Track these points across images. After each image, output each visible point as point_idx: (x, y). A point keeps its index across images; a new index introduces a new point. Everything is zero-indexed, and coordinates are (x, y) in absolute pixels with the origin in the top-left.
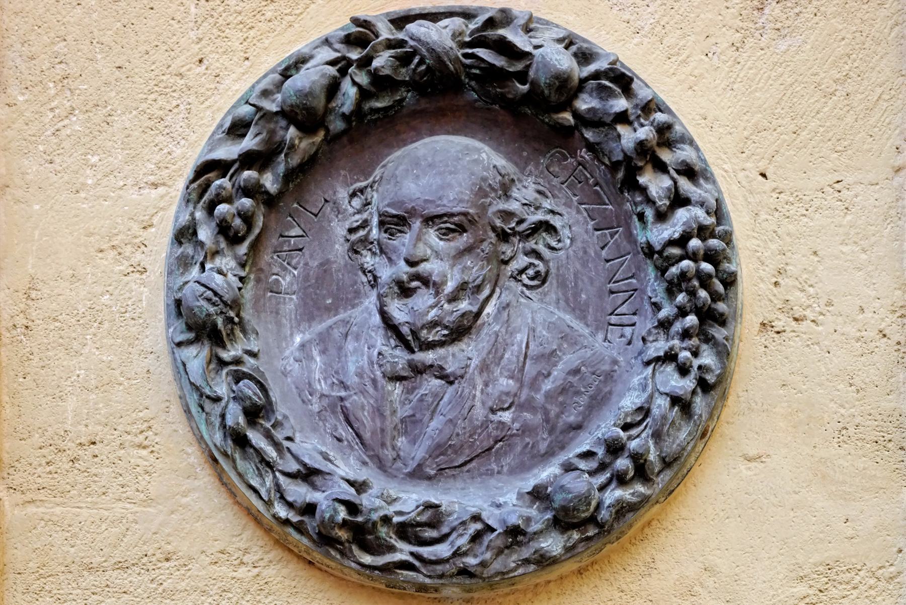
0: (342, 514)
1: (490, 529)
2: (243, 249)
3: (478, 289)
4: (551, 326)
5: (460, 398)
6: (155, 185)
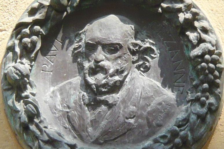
3: (122, 72)
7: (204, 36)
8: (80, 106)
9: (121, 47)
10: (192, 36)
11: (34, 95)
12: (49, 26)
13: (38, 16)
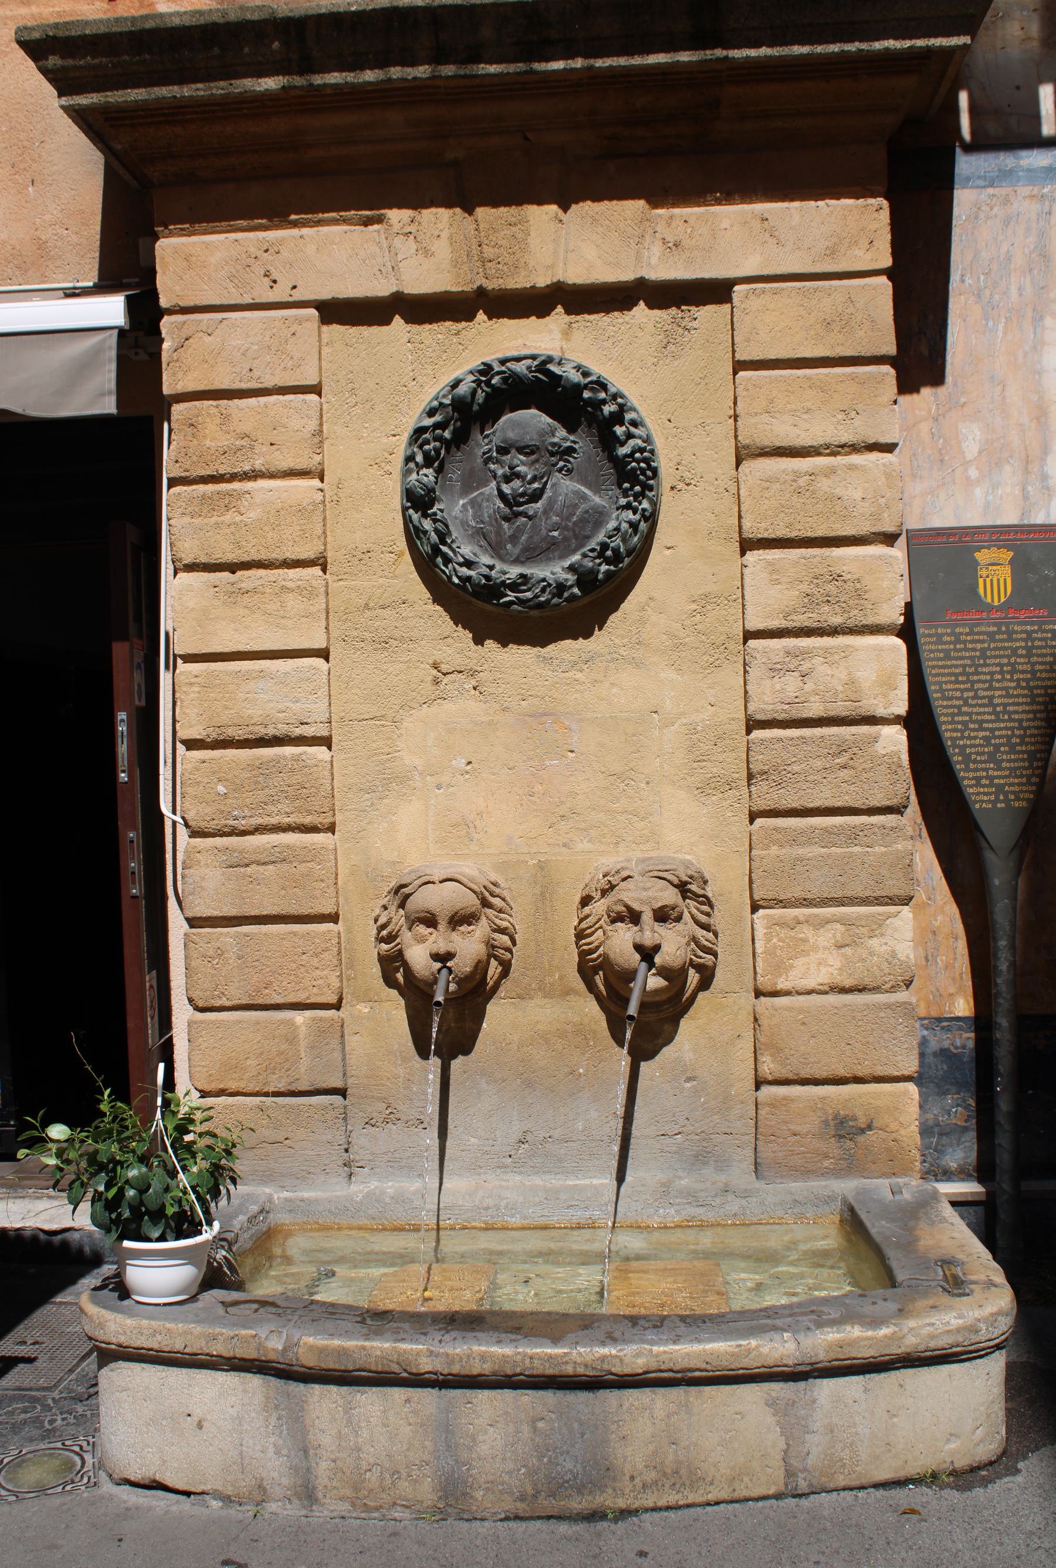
1: (549, 585)
3: (542, 477)
5: (533, 527)
6: (394, 435)
7: (632, 429)
8: (496, 520)
9: (538, 448)
10: (619, 430)
11: (442, 511)
13: (438, 418)
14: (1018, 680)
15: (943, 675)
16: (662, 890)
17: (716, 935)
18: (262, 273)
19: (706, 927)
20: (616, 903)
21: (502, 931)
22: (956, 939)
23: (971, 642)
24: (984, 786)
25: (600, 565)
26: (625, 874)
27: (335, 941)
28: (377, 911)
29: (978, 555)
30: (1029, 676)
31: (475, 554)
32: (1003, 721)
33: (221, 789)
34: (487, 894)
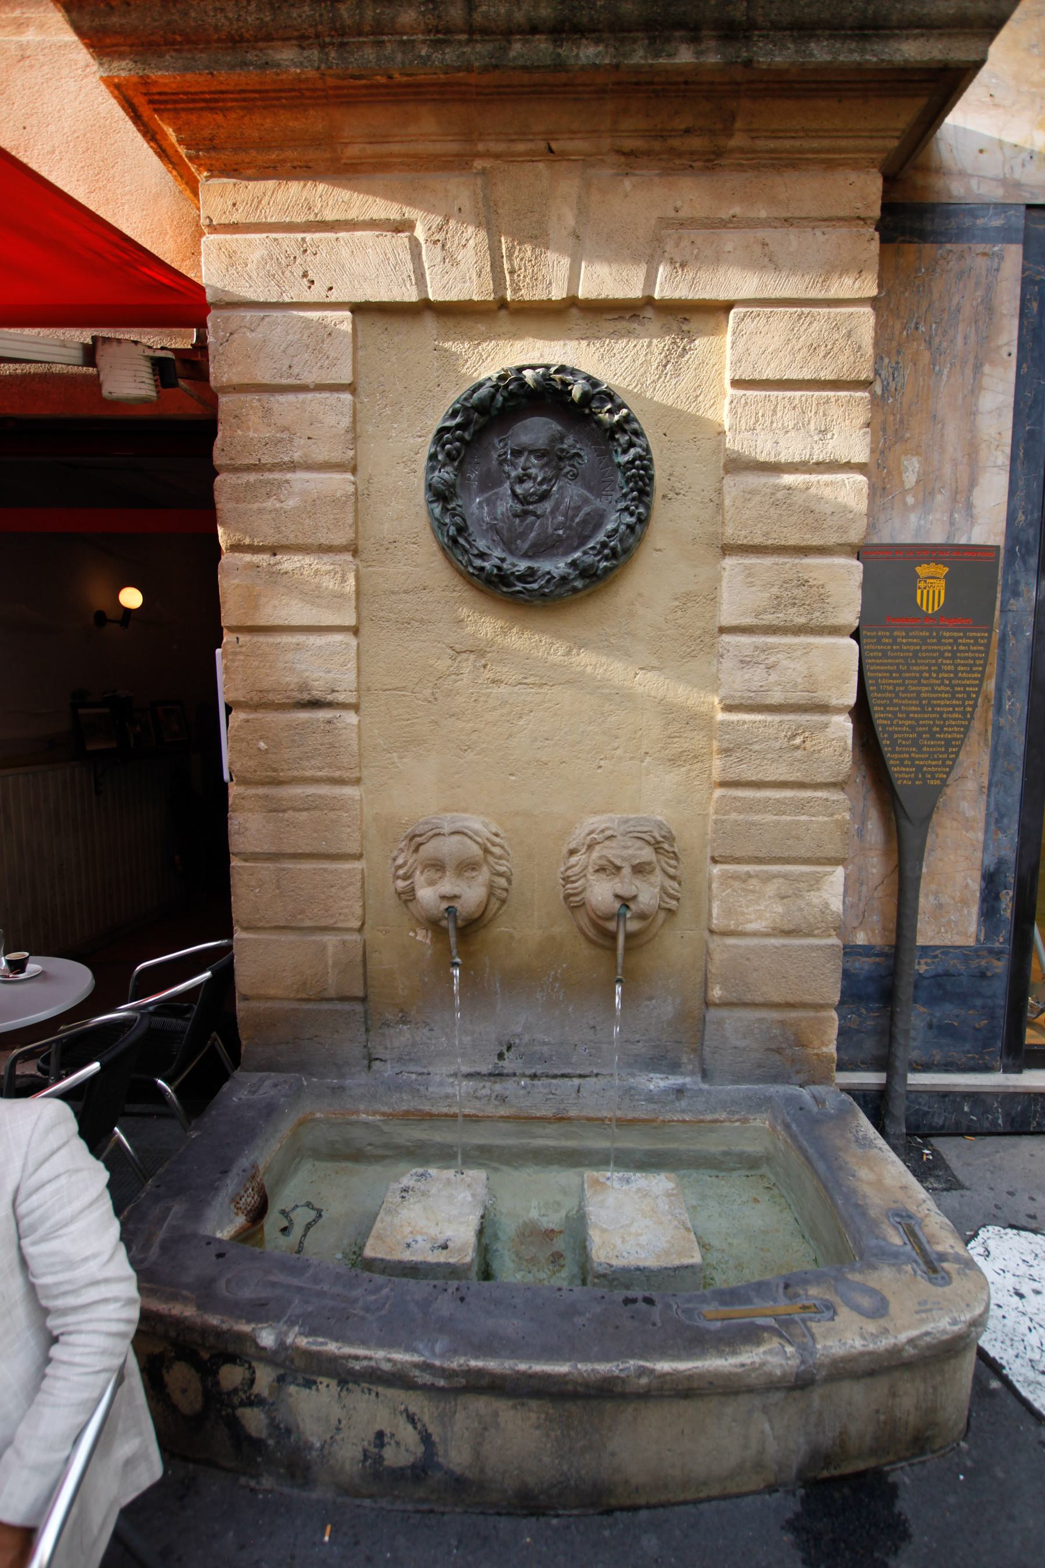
0: (495, 571)
1: (554, 578)
2: (456, 464)
3: (550, 480)
4: (579, 496)
5: (542, 525)
6: (420, 437)
7: (634, 439)
10: (624, 439)
12: (472, 430)
13: (458, 420)
14: (943, 679)
15: (880, 671)
16: (640, 849)
17: (680, 884)
18: (301, 274)
19: (673, 878)
20: (600, 858)
21: (500, 875)
22: (862, 884)
23: (906, 644)
24: (906, 766)
25: (599, 561)
26: (608, 833)
27: (358, 877)
28: (395, 853)
29: (918, 569)
30: (952, 675)
31: (489, 548)
32: (928, 712)
33: (262, 745)
34: (489, 845)
